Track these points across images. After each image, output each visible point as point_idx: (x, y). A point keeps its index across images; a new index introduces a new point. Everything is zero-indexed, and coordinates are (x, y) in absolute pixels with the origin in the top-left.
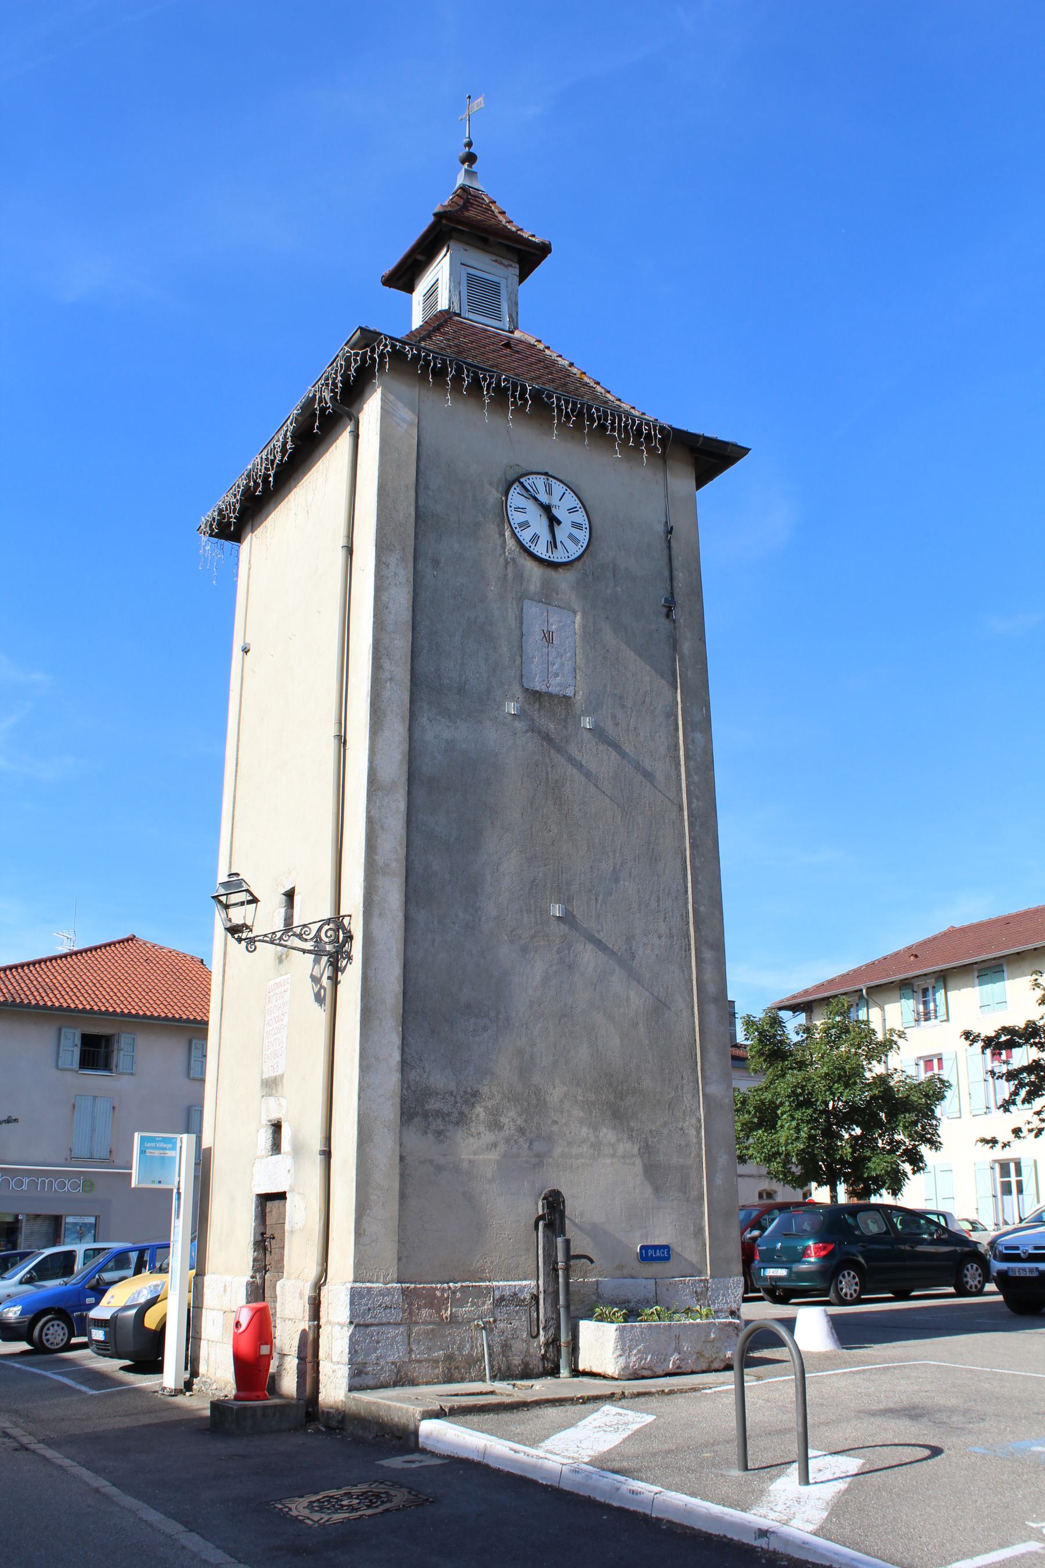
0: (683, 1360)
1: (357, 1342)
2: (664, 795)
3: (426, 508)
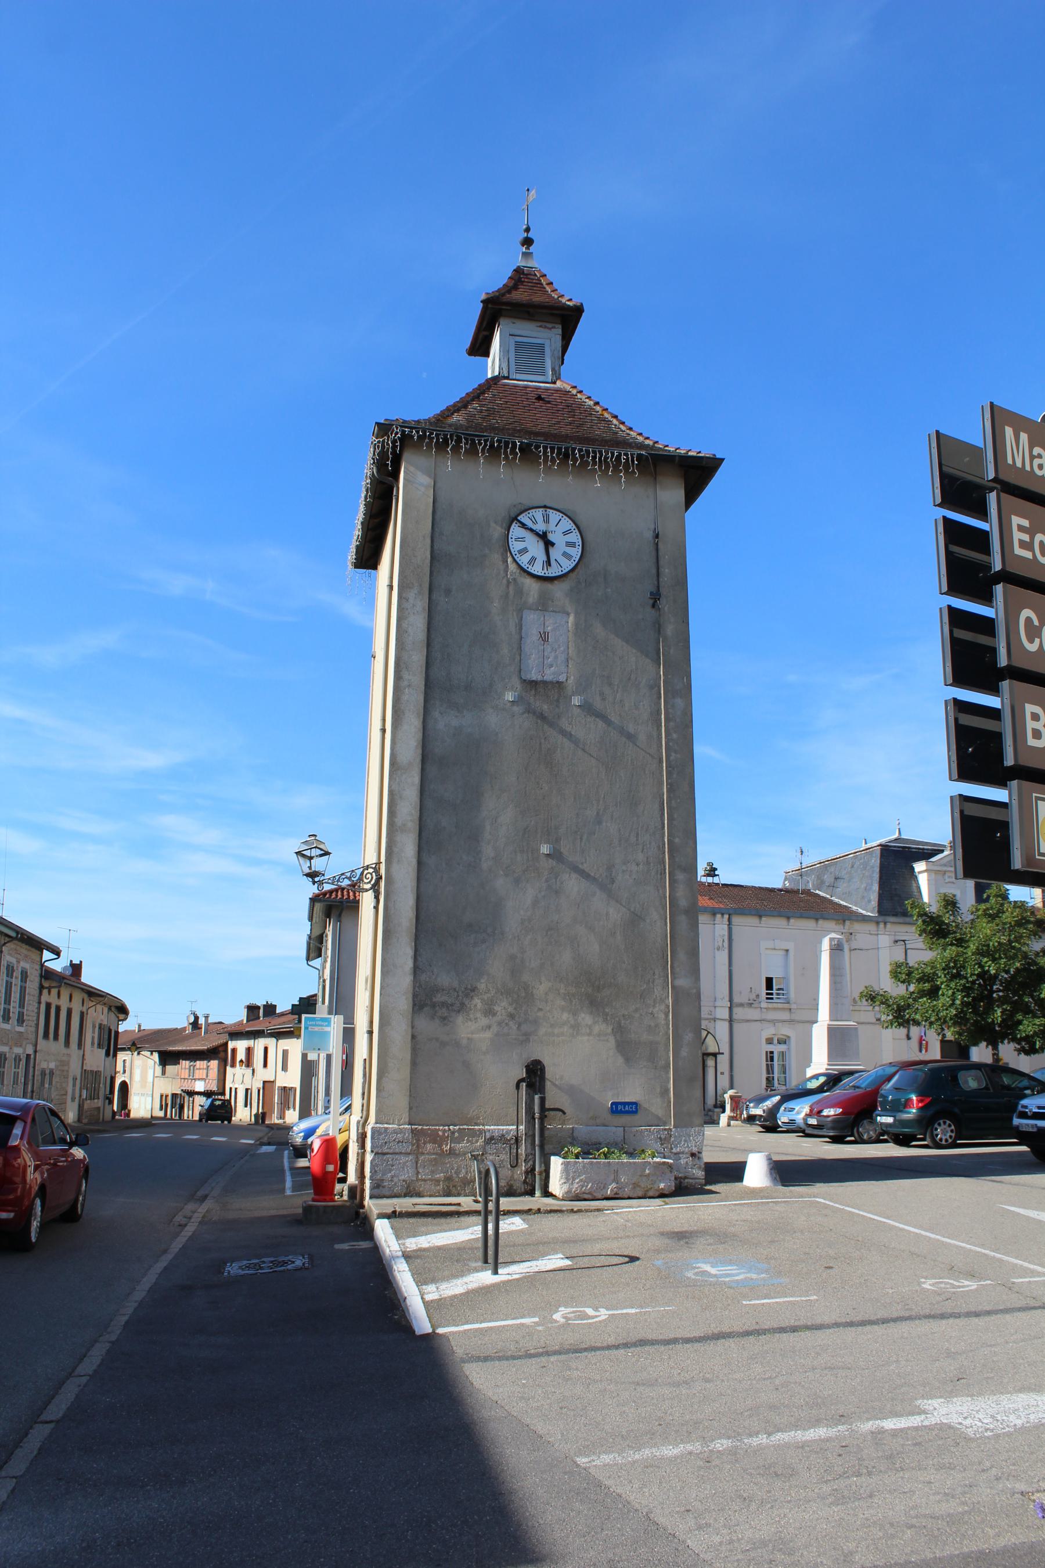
0: (621, 1188)
1: (377, 1165)
2: (646, 752)
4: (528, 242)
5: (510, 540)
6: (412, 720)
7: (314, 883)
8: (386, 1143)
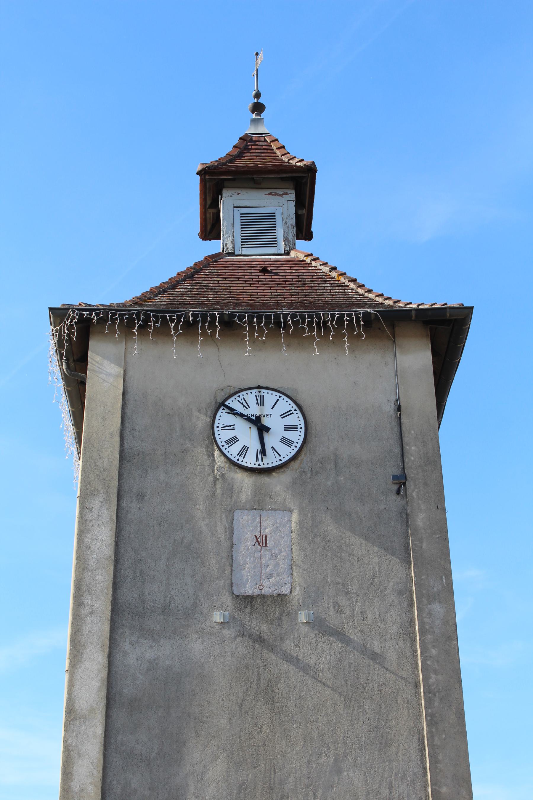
2: (397, 675)
3: (131, 449)
4: (258, 108)
5: (216, 429)
6: (95, 655)
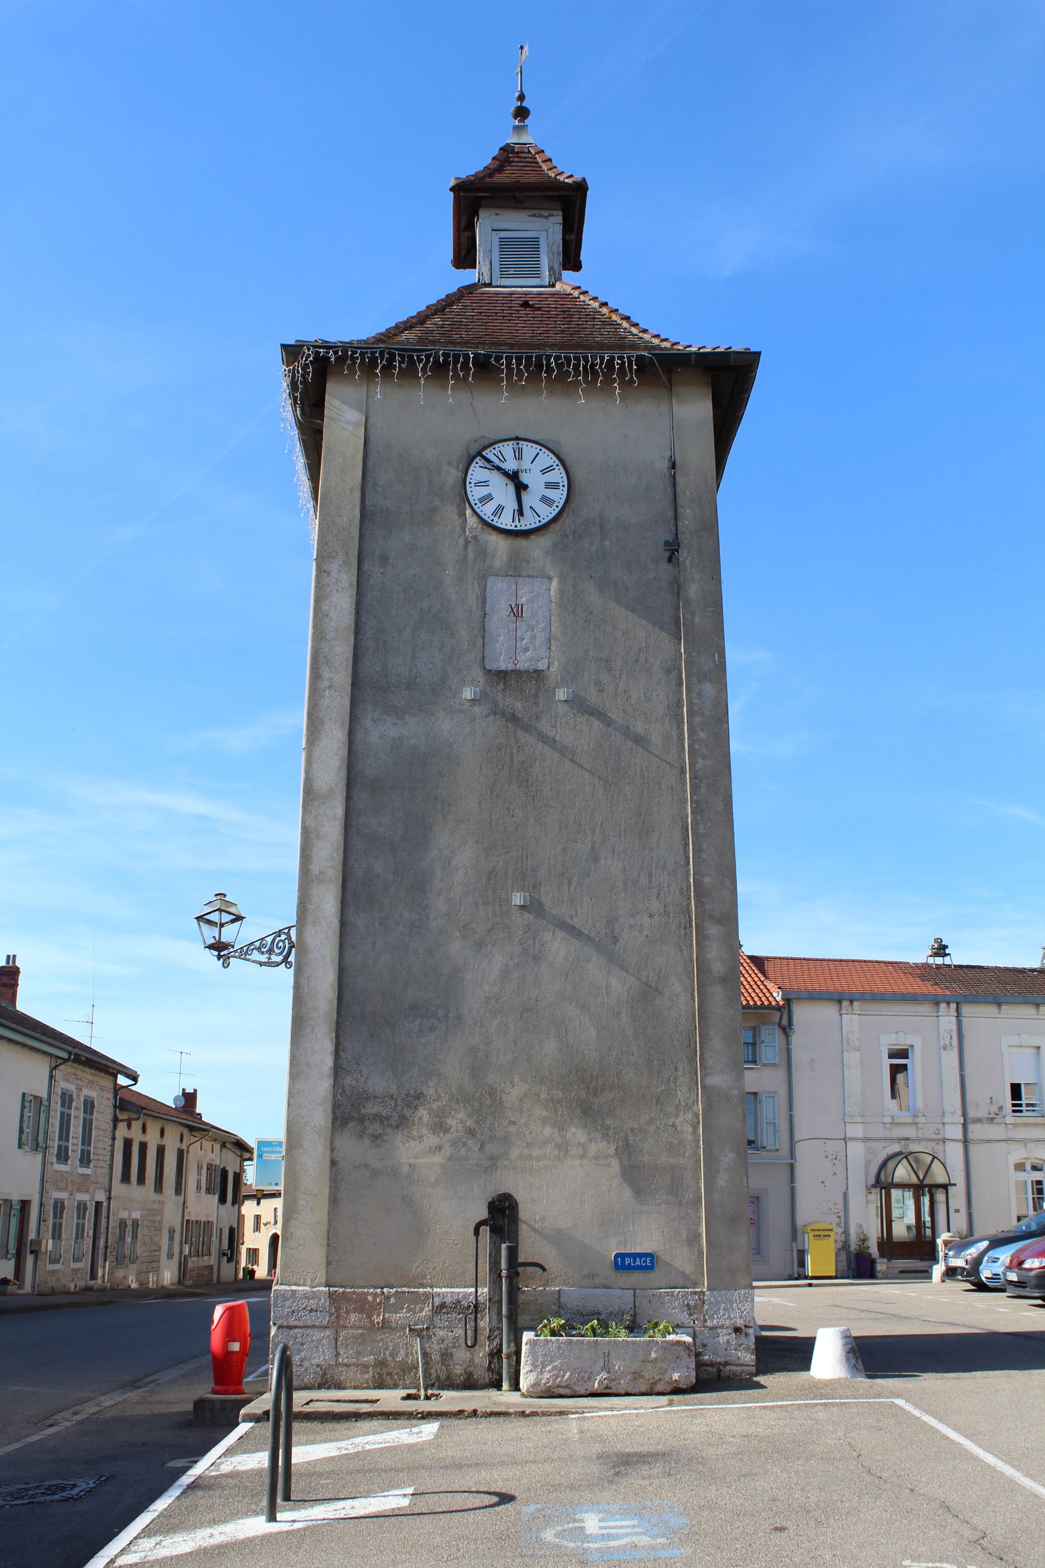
0: (614, 1380)
2: (661, 759)
3: (373, 506)
4: (522, 113)
7: (219, 957)
8: (293, 1312)
